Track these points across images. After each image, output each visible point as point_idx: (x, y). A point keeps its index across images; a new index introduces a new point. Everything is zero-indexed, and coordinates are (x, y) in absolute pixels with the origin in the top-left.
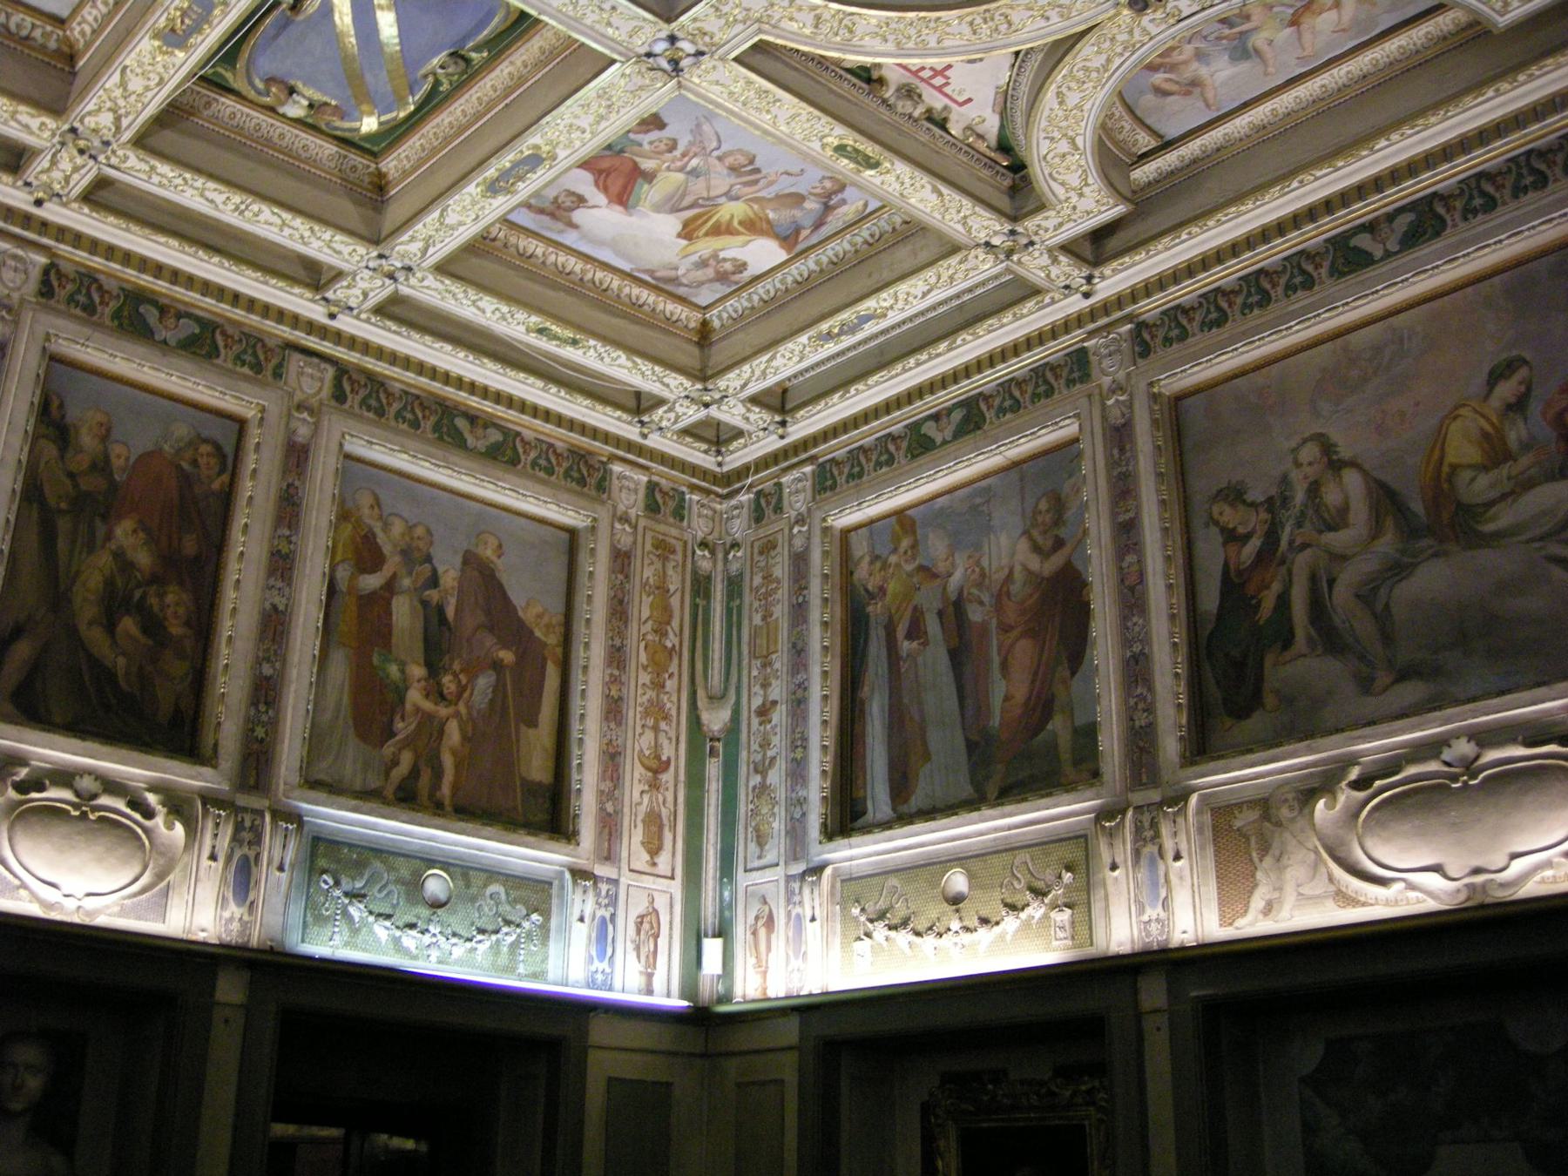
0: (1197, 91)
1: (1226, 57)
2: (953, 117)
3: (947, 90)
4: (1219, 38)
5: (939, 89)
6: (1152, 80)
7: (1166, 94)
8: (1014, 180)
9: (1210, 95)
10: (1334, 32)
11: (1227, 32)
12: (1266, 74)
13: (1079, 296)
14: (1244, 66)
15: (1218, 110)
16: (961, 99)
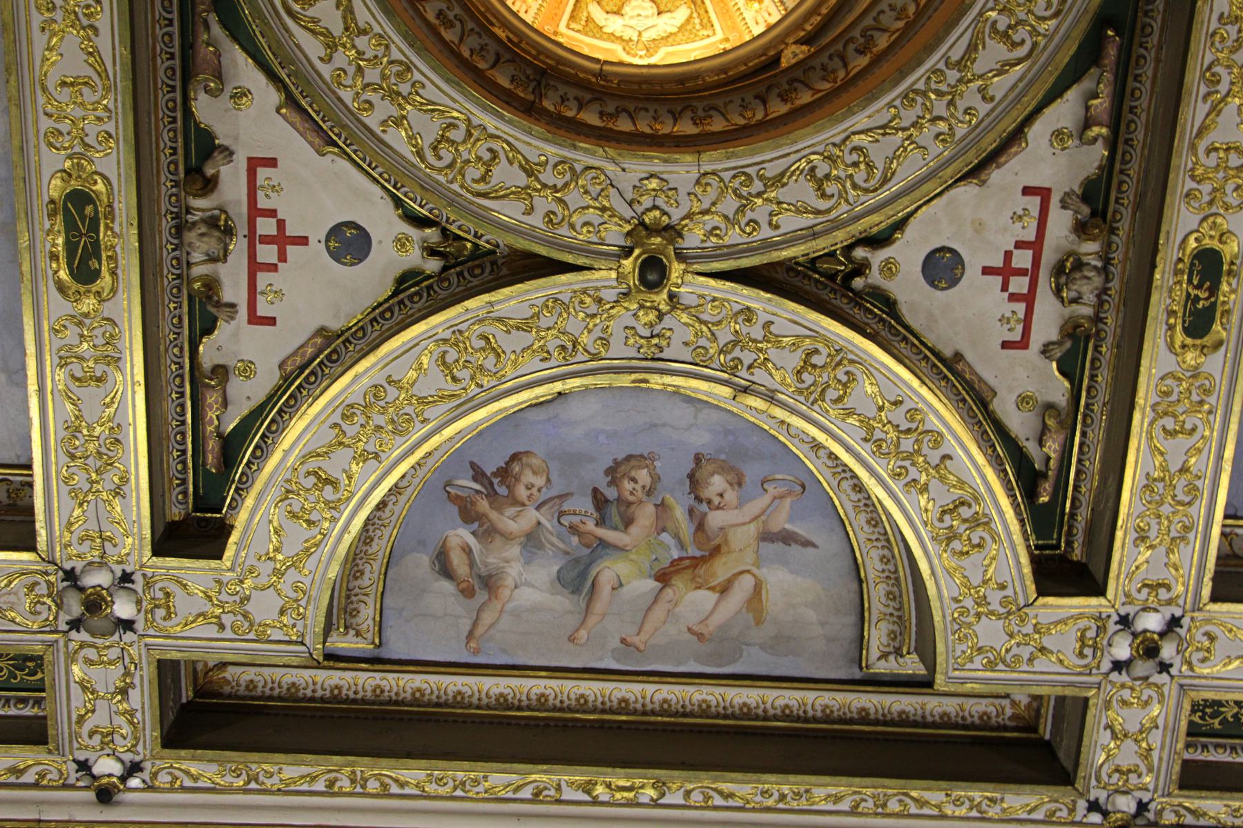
0: (482, 596)
1: (556, 568)
2: (224, 330)
3: (263, 279)
4: (573, 529)
5: (255, 267)
6: (451, 533)
7: (444, 569)
8: (188, 515)
9: (487, 618)
10: (689, 629)
11: (590, 525)
12: (571, 639)
13: (91, 795)
14: (562, 602)
15: (476, 652)
16: (262, 310)
